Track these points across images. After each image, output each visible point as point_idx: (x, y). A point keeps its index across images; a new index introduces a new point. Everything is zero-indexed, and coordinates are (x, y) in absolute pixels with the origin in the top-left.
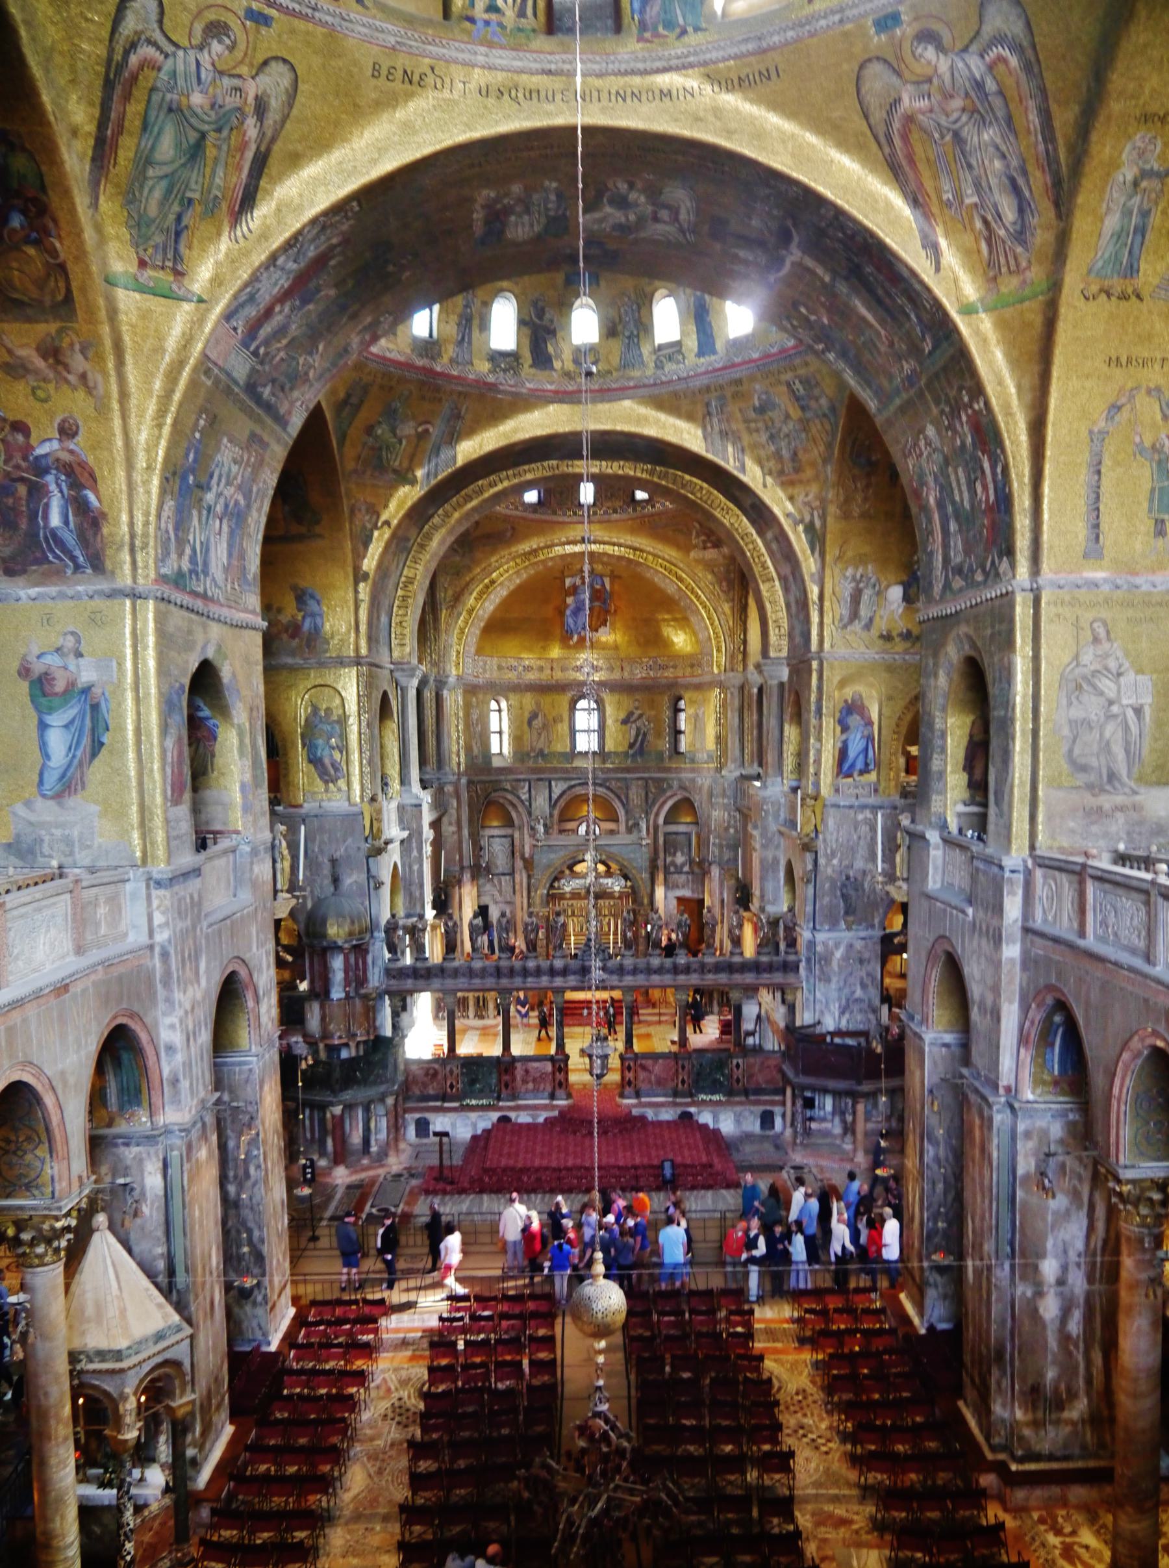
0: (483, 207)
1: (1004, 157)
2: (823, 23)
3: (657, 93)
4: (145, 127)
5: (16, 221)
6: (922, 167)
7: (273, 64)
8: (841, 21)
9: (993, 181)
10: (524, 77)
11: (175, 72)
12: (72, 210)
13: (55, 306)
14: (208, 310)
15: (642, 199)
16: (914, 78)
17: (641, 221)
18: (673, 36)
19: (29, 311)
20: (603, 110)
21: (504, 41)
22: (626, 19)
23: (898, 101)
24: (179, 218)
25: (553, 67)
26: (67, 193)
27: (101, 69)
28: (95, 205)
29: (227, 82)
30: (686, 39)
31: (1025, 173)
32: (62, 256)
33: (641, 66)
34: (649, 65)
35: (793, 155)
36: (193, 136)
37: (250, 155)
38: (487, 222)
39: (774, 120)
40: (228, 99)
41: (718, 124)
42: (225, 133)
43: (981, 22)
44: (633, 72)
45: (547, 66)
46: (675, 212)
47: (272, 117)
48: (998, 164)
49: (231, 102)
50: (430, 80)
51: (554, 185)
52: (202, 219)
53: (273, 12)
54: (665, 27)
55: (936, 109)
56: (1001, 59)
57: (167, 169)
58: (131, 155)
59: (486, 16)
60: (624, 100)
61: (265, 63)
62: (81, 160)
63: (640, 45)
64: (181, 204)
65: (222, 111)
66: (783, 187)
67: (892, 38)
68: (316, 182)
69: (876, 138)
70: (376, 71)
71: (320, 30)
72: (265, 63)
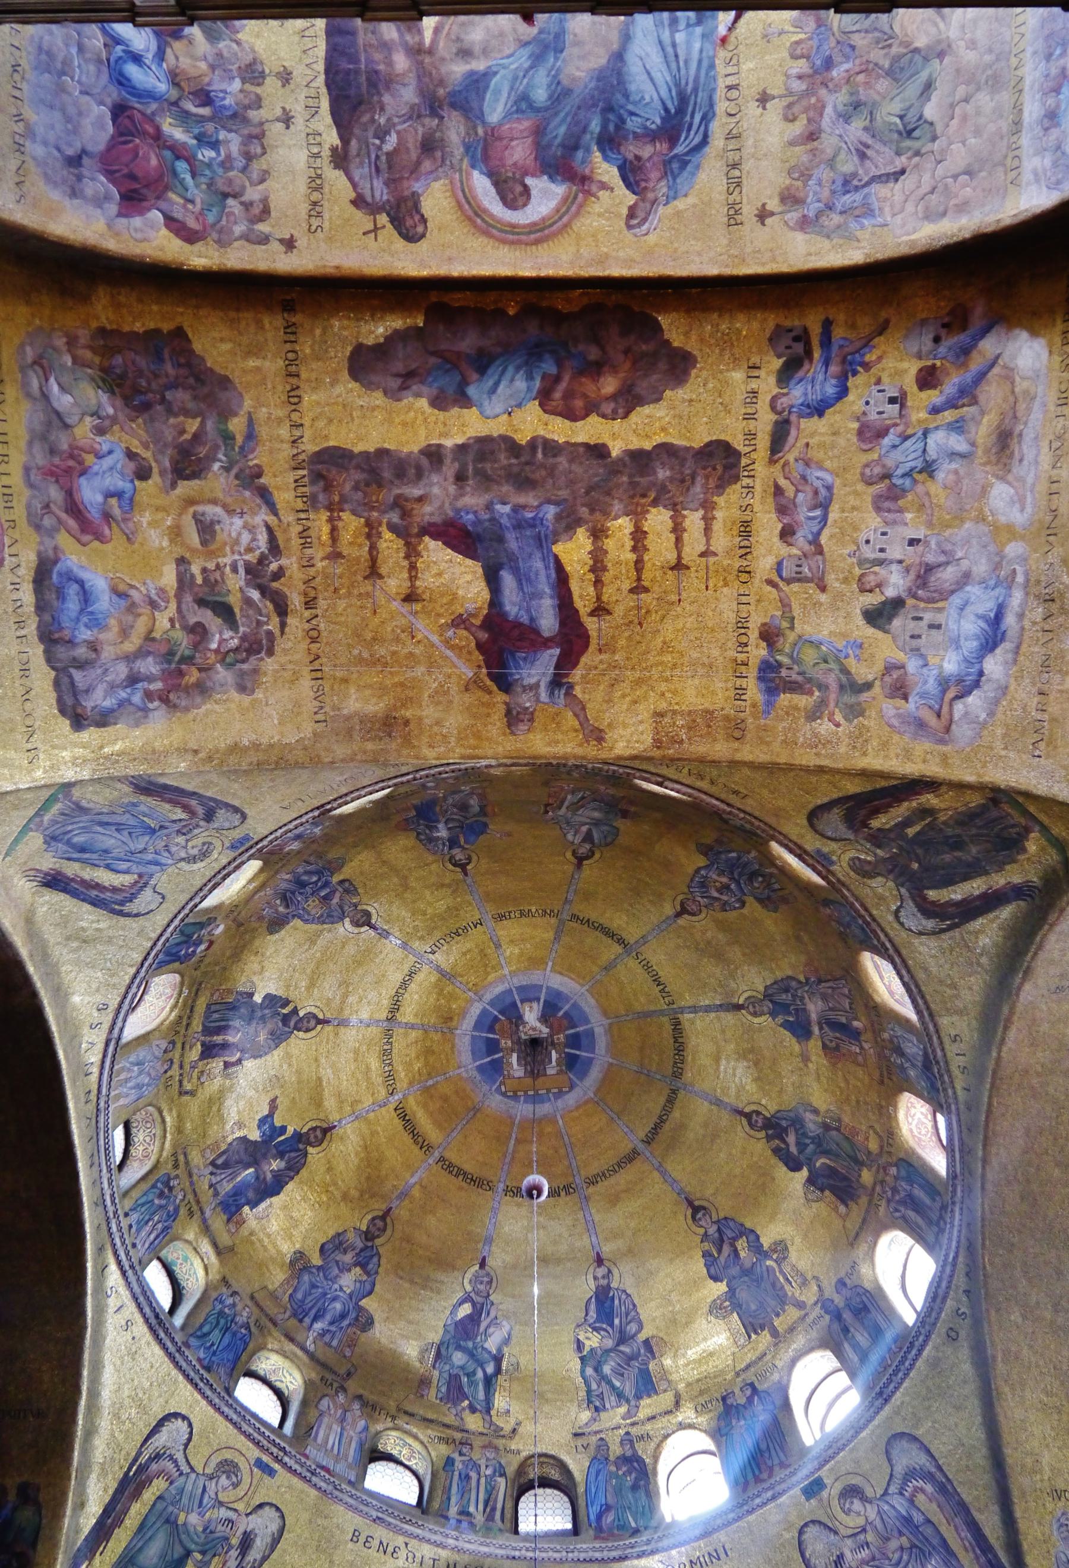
29: (223, 1513)
42: (207, 1558)
53: (276, 1466)
61: (261, 1506)
70: (355, 1537)
71: (313, 1492)
72: (261, 1506)
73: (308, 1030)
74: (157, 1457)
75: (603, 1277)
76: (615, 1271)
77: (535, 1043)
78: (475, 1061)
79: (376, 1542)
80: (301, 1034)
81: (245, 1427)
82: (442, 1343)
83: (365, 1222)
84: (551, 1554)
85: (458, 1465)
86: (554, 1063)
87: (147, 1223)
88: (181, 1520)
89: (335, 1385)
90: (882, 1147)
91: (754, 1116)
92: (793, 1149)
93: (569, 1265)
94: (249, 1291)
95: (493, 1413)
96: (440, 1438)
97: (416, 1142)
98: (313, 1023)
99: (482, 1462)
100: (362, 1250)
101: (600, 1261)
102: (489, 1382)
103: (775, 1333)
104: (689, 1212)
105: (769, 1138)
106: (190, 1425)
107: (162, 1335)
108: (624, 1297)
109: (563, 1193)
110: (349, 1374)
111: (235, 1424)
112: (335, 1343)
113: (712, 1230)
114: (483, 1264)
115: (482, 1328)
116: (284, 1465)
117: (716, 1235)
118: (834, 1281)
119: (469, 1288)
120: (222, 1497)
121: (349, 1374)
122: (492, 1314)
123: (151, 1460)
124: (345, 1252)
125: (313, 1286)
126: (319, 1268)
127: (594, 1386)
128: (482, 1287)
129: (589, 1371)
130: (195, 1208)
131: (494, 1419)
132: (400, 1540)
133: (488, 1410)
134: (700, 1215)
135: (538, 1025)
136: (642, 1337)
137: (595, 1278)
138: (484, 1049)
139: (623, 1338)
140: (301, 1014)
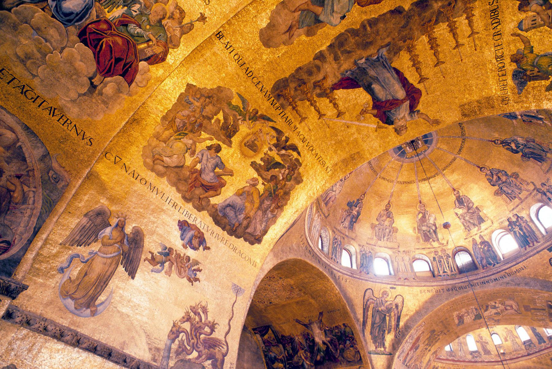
4: (372, 316)
5: (348, 342)
12: (360, 338)
13: (358, 361)
14: (393, 356)
15: (500, 305)
17: (502, 311)
19: (352, 363)
26: (358, 334)
27: (362, 307)
30: (495, 266)
32: (358, 349)
33: (486, 275)
34: (488, 274)
36: (383, 316)
37: (396, 317)
38: (458, 319)
44: (485, 277)
46: (512, 307)
47: (400, 308)
49: (390, 307)
51: (474, 307)
53: (395, 286)
54: (489, 265)
57: (378, 324)
62: (360, 326)
63: (484, 271)
70: (421, 292)
72: (396, 297)
73: (348, 177)
74: (368, 300)
75: (457, 194)
76: (460, 191)
78: (396, 154)
81: (383, 282)
85: (437, 259)
88: (380, 309)
89: (397, 252)
92: (514, 147)
93: (445, 194)
94: (365, 243)
95: (440, 240)
99: (443, 255)
102: (435, 232)
103: (520, 199)
104: (479, 169)
105: (503, 146)
106: (371, 289)
107: (355, 276)
109: (436, 176)
111: (381, 283)
112: (391, 240)
113: (489, 172)
114: (420, 202)
116: (397, 285)
117: (490, 173)
119: (419, 210)
120: (386, 300)
122: (428, 214)
123: (367, 302)
124: (383, 217)
125: (380, 229)
126: (378, 224)
128: (423, 208)
129: (462, 220)
130: (344, 236)
131: (441, 242)
133: (438, 240)
136: (474, 206)
137: (455, 195)
138: (398, 150)
139: (469, 208)
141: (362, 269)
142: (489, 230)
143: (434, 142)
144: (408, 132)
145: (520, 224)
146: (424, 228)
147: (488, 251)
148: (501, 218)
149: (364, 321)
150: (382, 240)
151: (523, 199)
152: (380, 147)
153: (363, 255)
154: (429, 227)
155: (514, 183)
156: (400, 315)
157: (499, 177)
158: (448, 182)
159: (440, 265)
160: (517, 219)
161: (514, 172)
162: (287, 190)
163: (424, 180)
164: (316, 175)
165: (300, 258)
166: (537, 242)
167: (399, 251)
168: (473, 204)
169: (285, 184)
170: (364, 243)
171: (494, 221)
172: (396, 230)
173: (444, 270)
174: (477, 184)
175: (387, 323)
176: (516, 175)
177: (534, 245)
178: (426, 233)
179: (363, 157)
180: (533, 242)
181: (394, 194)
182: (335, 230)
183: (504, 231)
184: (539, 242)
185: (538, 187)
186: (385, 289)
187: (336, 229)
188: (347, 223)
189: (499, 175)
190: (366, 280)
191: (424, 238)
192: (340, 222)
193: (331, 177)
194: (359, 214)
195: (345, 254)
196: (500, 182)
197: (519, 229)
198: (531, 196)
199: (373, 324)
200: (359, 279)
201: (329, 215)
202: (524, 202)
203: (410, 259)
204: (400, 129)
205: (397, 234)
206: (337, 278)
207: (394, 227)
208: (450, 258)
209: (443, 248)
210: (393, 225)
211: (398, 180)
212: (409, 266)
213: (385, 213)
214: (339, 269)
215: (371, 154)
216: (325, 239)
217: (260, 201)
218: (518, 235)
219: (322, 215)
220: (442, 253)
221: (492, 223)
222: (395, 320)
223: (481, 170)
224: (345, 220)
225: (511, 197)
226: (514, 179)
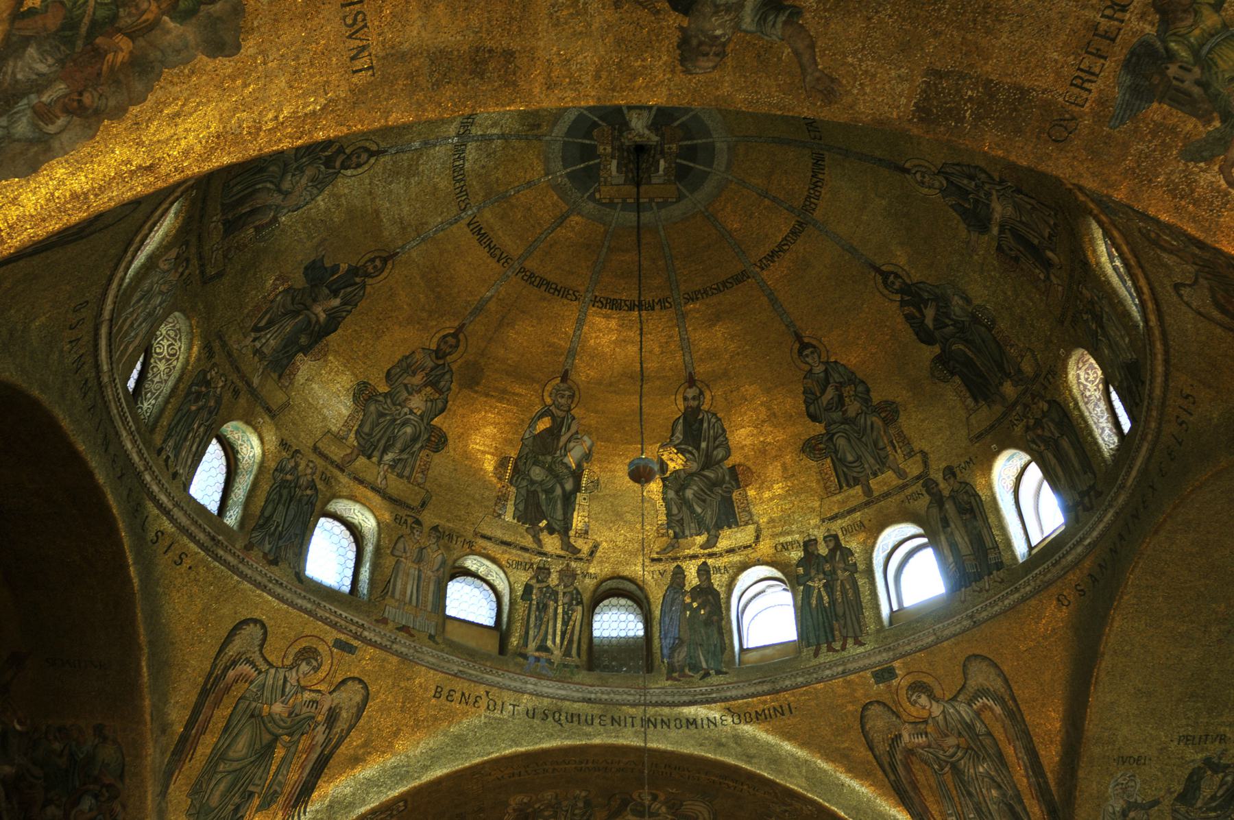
0: (514, 810)
1: (999, 787)
2: (828, 672)
3: (684, 721)
4: (226, 729)
5: (87, 803)
6: (925, 792)
7: (350, 683)
8: (844, 672)
9: (993, 808)
10: (567, 703)
11: (264, 685)
15: (664, 809)
16: (912, 719)
18: (698, 676)
20: (636, 734)
21: (550, 674)
22: (657, 662)
23: (899, 737)
24: (237, 808)
25: (593, 696)
27: (201, 680)
28: (164, 793)
29: (307, 696)
30: (708, 680)
31: (1021, 802)
33: (669, 699)
34: (676, 699)
35: (807, 778)
36: (267, 738)
37: (314, 756)
39: (788, 746)
40: (305, 709)
41: (739, 749)
42: (296, 737)
43: (966, 679)
44: (663, 704)
45: (589, 696)
47: (341, 726)
48: (994, 793)
50: (483, 703)
51: (584, 794)
52: (256, 812)
53: (355, 643)
55: (934, 745)
56: (985, 706)
57: (236, 765)
58: (208, 751)
59: (537, 654)
60: (655, 726)
62: (163, 753)
63: (669, 682)
64: (242, 797)
65: (298, 718)
66: (798, 805)
67: (889, 687)
68: (370, 783)
69: (881, 766)
72: (343, 682)
73: (359, 166)
75: (694, 398)
76: (708, 395)
77: (640, 149)
78: (565, 167)
79: (458, 695)
80: (349, 172)
81: (320, 613)
82: (519, 458)
83: (435, 340)
84: (625, 696)
86: (661, 172)
87: (185, 439)
89: (410, 520)
90: (1037, 376)
91: (892, 278)
92: (929, 322)
93: (658, 383)
94: (310, 443)
95: (572, 533)
96: (518, 563)
97: (492, 255)
98: (364, 156)
100: (432, 370)
101: (691, 382)
103: (868, 491)
104: (797, 345)
105: (903, 303)
106: (263, 626)
107: (221, 552)
108: (713, 420)
109: (657, 307)
110: (423, 504)
112: (406, 473)
113: (819, 369)
114: (565, 377)
115: (561, 444)
118: (944, 465)
119: (548, 401)
121: (423, 504)
122: (574, 429)
124: (414, 374)
125: (382, 415)
126: (386, 395)
127: (675, 511)
128: (562, 401)
129: (671, 494)
130: (240, 384)
131: (572, 540)
132: (481, 690)
134: (807, 352)
135: (647, 132)
137: (685, 399)
140: (348, 151)
141: (257, 536)
142: (736, 558)
143: (708, 187)
144: (716, 75)
145: (834, 572)
146: (537, 473)
147: (708, 623)
148: (788, 534)
149: (184, 739)
150: (375, 459)
151: (876, 494)
152: (597, 77)
153: (283, 484)
154: (557, 476)
155: (875, 433)
156: (332, 753)
157: (841, 397)
158: (686, 345)
159: (539, 619)
160: (832, 552)
161: (891, 398)
162: (154, 55)
163: (614, 305)
164: (305, 58)
165: (36, 393)
166: (859, 643)
167: (418, 522)
168: (728, 453)
169: (154, 25)
170: (305, 442)
171: (765, 533)
172: (438, 441)
173: (545, 639)
174: (768, 391)
175: (274, 768)
176: (890, 413)
177: (843, 648)
178: (535, 492)
179: (515, 84)
180: (845, 639)
181: (492, 306)
182: (216, 345)
183: (779, 574)
184: (863, 644)
185: (933, 475)
186: (314, 643)
187: (224, 345)
188: (271, 341)
189: (848, 391)
190: (258, 585)
191: (521, 507)
192: (250, 324)
193: (358, 97)
194: (334, 321)
195: (214, 457)
196: (836, 416)
197: (825, 585)
198: (902, 496)
199: (218, 756)
200: (234, 570)
201: (220, 275)
202: (875, 507)
203: (444, 563)
204: (701, 44)
205: (437, 458)
206: (151, 535)
207: (434, 427)
208: (580, 608)
209: (573, 564)
210: (436, 421)
211: (531, 264)
212: (432, 587)
213: (429, 364)
214: (170, 505)
215: (550, 86)
216: (162, 366)
217: (8, 36)
218: (814, 602)
219: (195, 262)
220: (561, 579)
221: (757, 537)
222: (303, 767)
223: (800, 353)
224: (271, 323)
225: (847, 476)
226: (880, 423)
